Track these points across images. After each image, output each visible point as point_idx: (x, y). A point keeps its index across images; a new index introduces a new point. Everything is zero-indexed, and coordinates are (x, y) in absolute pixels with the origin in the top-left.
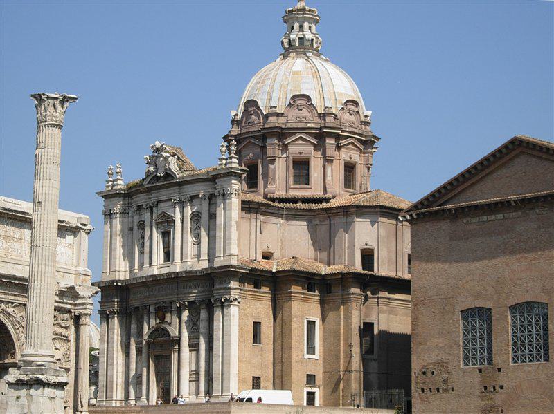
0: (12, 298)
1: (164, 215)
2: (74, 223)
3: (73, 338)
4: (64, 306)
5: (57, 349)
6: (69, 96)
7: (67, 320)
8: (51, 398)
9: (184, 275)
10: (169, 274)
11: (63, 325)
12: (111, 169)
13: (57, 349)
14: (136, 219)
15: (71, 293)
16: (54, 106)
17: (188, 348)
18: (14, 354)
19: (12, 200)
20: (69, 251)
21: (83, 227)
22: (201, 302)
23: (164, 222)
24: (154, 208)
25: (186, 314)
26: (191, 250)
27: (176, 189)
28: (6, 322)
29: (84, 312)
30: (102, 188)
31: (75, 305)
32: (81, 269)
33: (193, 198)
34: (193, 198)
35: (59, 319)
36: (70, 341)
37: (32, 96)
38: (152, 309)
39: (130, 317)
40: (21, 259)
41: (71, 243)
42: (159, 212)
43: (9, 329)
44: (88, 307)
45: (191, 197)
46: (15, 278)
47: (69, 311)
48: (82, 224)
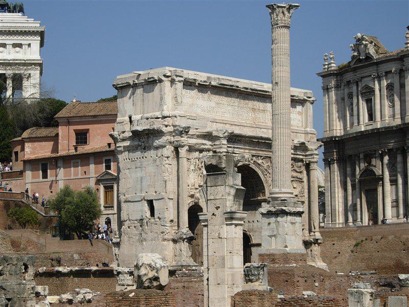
0: (261, 152)
1: (367, 87)
2: (302, 97)
3: (305, 179)
4: (298, 156)
5: (294, 188)
6: (293, 4)
7: (300, 167)
8: (292, 223)
9: (383, 130)
10: (373, 130)
12: (326, 56)
13: (294, 188)
14: (347, 91)
15: (302, 147)
16: (283, 12)
17: (389, 184)
18: (264, 193)
19: (256, 83)
20: (299, 117)
21: (309, 99)
22: (397, 149)
23: (367, 92)
24: (359, 83)
25: (386, 159)
26: (387, 111)
27: (375, 67)
28: (257, 170)
29: (313, 160)
30: (321, 70)
31: (306, 156)
32: (308, 129)
33: (387, 73)
34: (387, 73)
35: (295, 166)
36: (304, 182)
37: (267, 6)
38: (361, 156)
39: (346, 163)
40: (266, 124)
41: (301, 111)
42: (363, 85)
44: (315, 156)
45: (385, 72)
46: (262, 138)
47: (302, 161)
48: (307, 97)
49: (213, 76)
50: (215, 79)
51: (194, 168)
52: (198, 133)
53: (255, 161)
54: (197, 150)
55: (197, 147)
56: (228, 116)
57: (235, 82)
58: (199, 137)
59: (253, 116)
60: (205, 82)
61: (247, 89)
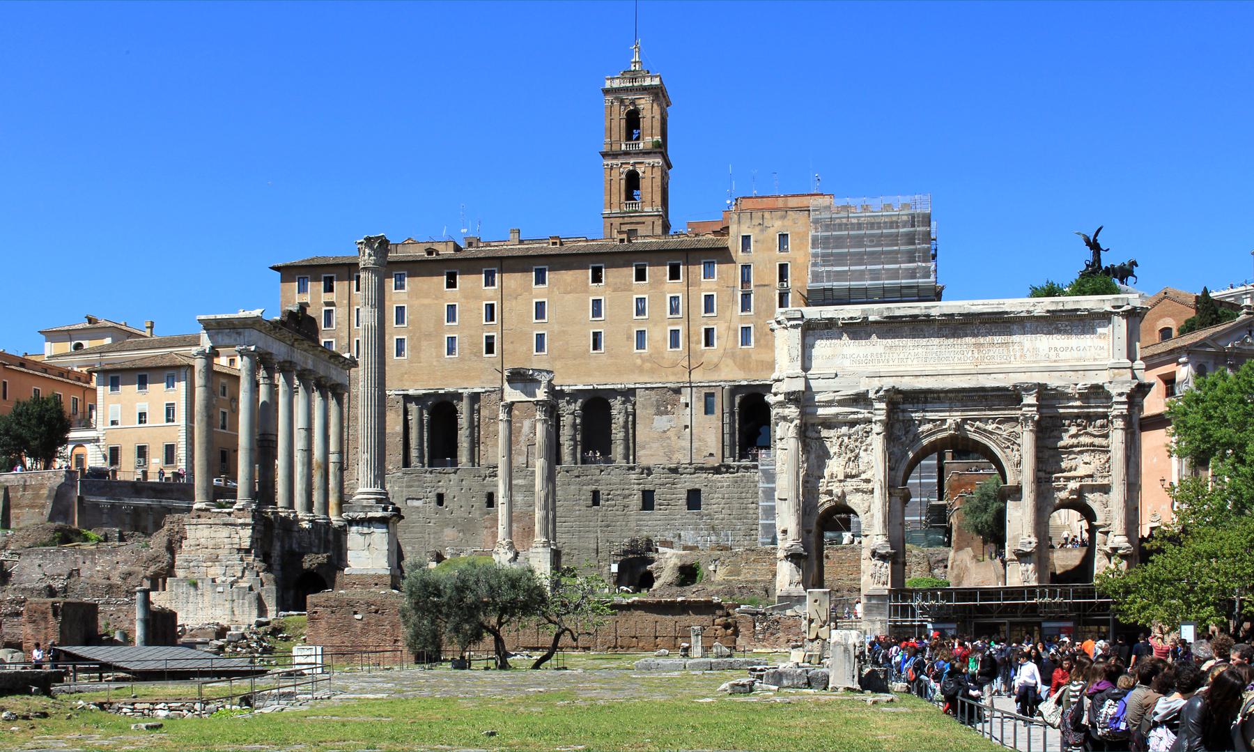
5: (1086, 463)
11: (1096, 433)
13: (1086, 463)
19: (986, 301)
46: (983, 389)
50: (880, 312)
52: (837, 398)
53: (977, 428)
54: (845, 424)
56: (915, 362)
57: (926, 308)
58: (842, 403)
59: (976, 355)
60: (851, 318)
61: (952, 315)
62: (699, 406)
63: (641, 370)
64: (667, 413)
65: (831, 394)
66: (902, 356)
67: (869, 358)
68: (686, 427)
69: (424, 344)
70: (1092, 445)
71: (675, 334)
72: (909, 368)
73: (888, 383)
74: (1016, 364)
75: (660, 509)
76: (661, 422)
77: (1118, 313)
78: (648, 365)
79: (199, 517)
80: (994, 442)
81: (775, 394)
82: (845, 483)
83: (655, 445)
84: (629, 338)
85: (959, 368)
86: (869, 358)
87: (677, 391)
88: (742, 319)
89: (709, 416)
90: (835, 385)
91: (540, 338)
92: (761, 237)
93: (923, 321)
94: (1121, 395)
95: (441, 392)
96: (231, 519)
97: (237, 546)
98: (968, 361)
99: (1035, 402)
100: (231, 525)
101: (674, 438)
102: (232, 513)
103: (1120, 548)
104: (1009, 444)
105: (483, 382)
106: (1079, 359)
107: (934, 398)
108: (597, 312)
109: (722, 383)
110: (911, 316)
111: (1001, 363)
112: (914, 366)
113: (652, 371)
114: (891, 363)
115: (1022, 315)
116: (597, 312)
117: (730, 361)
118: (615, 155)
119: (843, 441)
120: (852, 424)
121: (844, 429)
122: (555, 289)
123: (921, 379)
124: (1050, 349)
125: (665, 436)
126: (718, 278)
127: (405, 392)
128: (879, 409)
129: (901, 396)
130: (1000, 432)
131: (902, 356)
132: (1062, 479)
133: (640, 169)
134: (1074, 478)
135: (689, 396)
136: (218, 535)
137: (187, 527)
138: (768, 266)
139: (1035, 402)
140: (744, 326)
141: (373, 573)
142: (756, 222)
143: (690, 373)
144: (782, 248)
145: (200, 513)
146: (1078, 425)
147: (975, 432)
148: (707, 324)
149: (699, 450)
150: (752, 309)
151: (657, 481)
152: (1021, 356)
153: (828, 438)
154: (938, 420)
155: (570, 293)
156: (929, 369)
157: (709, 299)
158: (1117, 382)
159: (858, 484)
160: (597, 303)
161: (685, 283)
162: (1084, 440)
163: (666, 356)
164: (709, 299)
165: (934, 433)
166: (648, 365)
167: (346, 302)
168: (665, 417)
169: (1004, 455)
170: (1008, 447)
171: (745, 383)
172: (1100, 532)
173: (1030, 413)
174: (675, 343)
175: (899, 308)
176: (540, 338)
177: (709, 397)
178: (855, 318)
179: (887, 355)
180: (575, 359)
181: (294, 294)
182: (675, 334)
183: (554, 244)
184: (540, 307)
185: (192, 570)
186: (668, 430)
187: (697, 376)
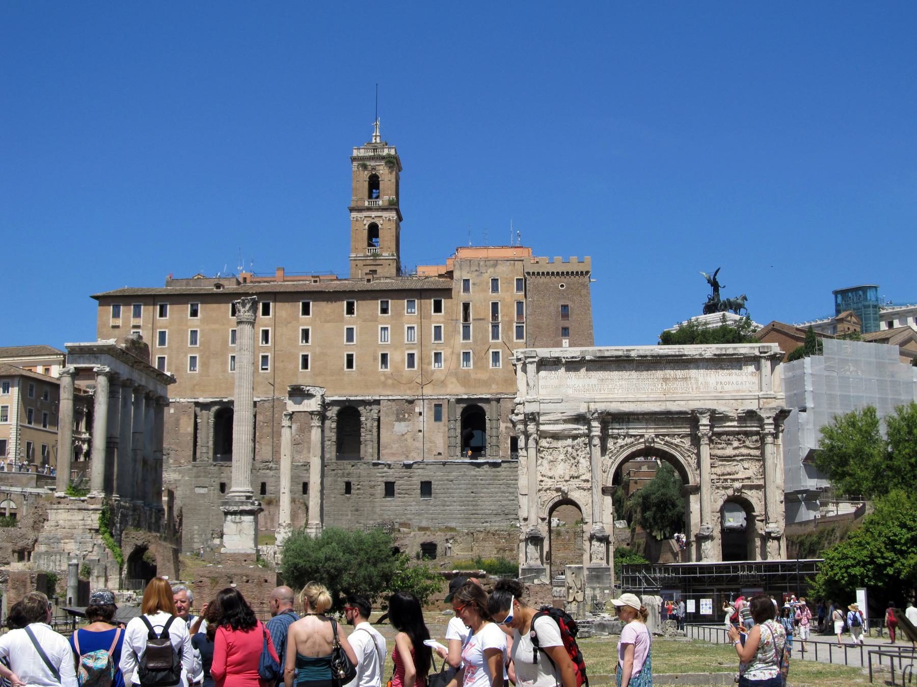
0: (680, 430)
5: (745, 469)
11: (752, 446)
13: (745, 469)
40: (690, 395)
43: (678, 457)
46: (669, 413)
49: (590, 349)
51: (564, 458)
53: (667, 442)
54: (569, 437)
55: (566, 432)
57: (627, 350)
58: (566, 421)
60: (573, 357)
61: (646, 356)
62: (429, 414)
63: (384, 385)
64: (404, 420)
65: (561, 415)
66: (610, 386)
67: (586, 388)
68: (420, 431)
69: (212, 361)
70: (749, 455)
71: (411, 356)
72: (615, 396)
73: (601, 407)
74: (694, 394)
75: (399, 497)
76: (401, 427)
77: (765, 357)
78: (390, 381)
79: (59, 503)
80: (679, 452)
81: (517, 415)
82: (569, 482)
83: (395, 446)
84: (375, 359)
85: (653, 396)
86: (586, 388)
87: (411, 402)
88: (464, 346)
89: (438, 423)
90: (561, 408)
91: (305, 359)
92: (477, 281)
93: (625, 360)
94: (768, 418)
95: (225, 400)
96: (84, 505)
97: (89, 527)
98: (659, 391)
99: (708, 423)
100: (85, 509)
101: (410, 440)
102: (85, 500)
103: (773, 533)
104: (690, 454)
105: (259, 393)
106: (738, 391)
107: (634, 419)
108: (350, 338)
109: (448, 397)
110: (616, 357)
111: (682, 393)
112: (619, 394)
113: (393, 386)
114: (602, 392)
115: (697, 357)
116: (350, 338)
117: (454, 380)
118: (360, 210)
119: (567, 451)
120: (575, 437)
121: (569, 441)
122: (317, 319)
123: (625, 404)
124: (717, 383)
125: (403, 438)
126: (445, 313)
127: (196, 400)
128: (595, 427)
129: (610, 417)
130: (683, 445)
131: (610, 386)
132: (729, 481)
133: (379, 222)
134: (737, 480)
135: (421, 407)
136: (73, 518)
137: (49, 511)
138: (483, 304)
139: (708, 423)
140: (465, 351)
141: (243, 552)
142: (474, 268)
143: (422, 388)
144: (495, 288)
145: (59, 500)
146: (739, 440)
147: (664, 444)
148: (436, 349)
149: (430, 450)
150: (471, 338)
151: (397, 475)
152: (697, 388)
153: (556, 448)
154: (638, 435)
155: (329, 322)
156: (631, 397)
157: (438, 329)
158: (766, 409)
159: (579, 483)
160: (350, 331)
161: (419, 316)
162: (744, 451)
163: (404, 374)
164: (438, 329)
165: (635, 445)
166: (390, 381)
167: (150, 326)
168: (403, 424)
169: (686, 462)
170: (689, 456)
171: (466, 397)
172: (758, 520)
173: (705, 431)
174: (411, 364)
175: (608, 350)
176: (305, 359)
177: (438, 407)
178: (576, 358)
179: (600, 387)
180: (332, 376)
181: (109, 319)
182: (411, 356)
183: (315, 281)
184: (306, 333)
185: (52, 545)
186: (406, 433)
187: (428, 391)
